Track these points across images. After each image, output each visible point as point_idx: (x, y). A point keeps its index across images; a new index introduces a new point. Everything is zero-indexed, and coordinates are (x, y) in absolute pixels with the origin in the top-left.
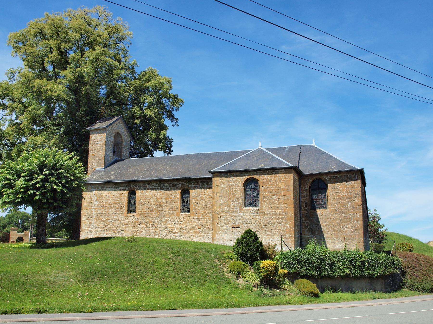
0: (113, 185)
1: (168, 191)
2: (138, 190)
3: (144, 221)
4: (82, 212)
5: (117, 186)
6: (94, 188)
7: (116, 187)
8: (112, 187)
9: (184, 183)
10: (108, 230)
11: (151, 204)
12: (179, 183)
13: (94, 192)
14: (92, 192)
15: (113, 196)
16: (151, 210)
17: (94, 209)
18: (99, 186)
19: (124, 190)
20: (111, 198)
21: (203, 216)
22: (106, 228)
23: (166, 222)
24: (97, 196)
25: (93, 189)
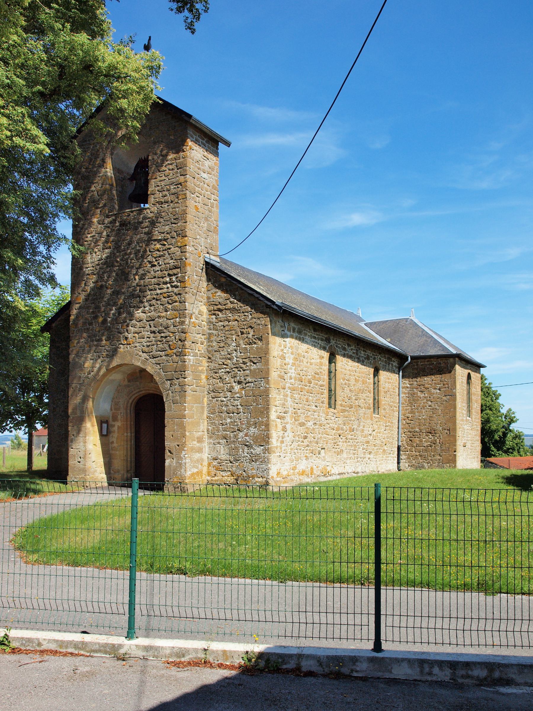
0: (312, 331)
1: (363, 367)
2: (338, 355)
3: (344, 427)
4: (270, 396)
5: (317, 335)
6: (289, 330)
7: (315, 338)
8: (312, 337)
9: (376, 355)
10: (308, 448)
11: (350, 390)
12: (373, 354)
13: (288, 340)
14: (285, 339)
15: (312, 361)
16: (351, 404)
17: (289, 388)
18: (295, 326)
19: (324, 349)
20: (311, 364)
21: (389, 422)
22: (306, 442)
23: (363, 431)
24: (292, 353)
25: (286, 331)
